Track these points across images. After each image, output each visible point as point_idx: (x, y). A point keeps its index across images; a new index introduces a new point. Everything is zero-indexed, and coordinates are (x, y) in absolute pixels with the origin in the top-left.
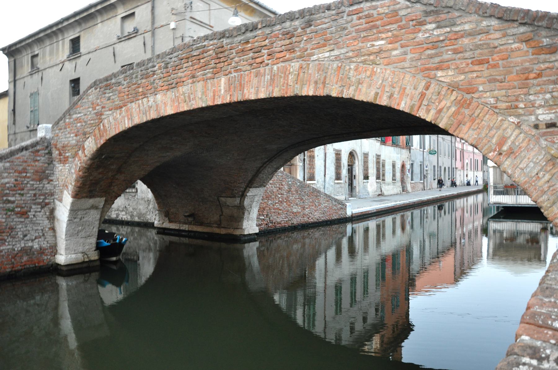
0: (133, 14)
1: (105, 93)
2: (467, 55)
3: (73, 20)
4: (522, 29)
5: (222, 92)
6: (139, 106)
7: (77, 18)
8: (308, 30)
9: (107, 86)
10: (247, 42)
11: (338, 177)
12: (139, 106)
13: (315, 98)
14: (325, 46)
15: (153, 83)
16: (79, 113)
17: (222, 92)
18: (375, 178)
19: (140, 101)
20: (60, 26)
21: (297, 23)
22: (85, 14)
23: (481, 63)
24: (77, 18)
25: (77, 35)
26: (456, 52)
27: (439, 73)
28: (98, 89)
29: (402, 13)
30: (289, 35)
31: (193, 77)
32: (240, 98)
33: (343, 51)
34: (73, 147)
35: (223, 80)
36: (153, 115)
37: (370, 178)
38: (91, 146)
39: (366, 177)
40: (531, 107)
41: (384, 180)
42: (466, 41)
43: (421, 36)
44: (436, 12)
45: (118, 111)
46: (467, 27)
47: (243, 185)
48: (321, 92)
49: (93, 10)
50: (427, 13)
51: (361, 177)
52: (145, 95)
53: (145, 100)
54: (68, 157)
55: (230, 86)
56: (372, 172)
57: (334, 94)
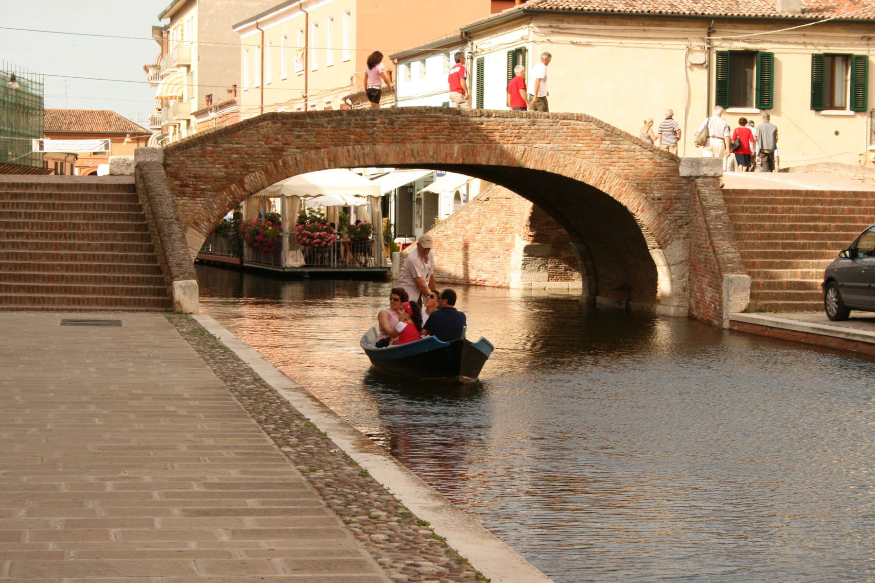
1: (292, 131)
2: (625, 160)
4: (649, 153)
5: (456, 155)
6: (348, 151)
8: (533, 127)
9: (297, 124)
12: (348, 151)
13: (534, 170)
14: (543, 139)
15: (372, 134)
16: (237, 143)
17: (456, 155)
19: (351, 147)
21: (525, 120)
26: (620, 158)
27: (611, 168)
28: (279, 125)
29: (593, 131)
31: (425, 138)
32: (472, 162)
33: (557, 145)
34: (216, 179)
35: (456, 146)
42: (624, 153)
43: (602, 147)
44: (611, 136)
45: (312, 152)
46: (626, 147)
50: (607, 136)
52: (358, 142)
53: (358, 147)
55: (463, 151)
57: (548, 170)
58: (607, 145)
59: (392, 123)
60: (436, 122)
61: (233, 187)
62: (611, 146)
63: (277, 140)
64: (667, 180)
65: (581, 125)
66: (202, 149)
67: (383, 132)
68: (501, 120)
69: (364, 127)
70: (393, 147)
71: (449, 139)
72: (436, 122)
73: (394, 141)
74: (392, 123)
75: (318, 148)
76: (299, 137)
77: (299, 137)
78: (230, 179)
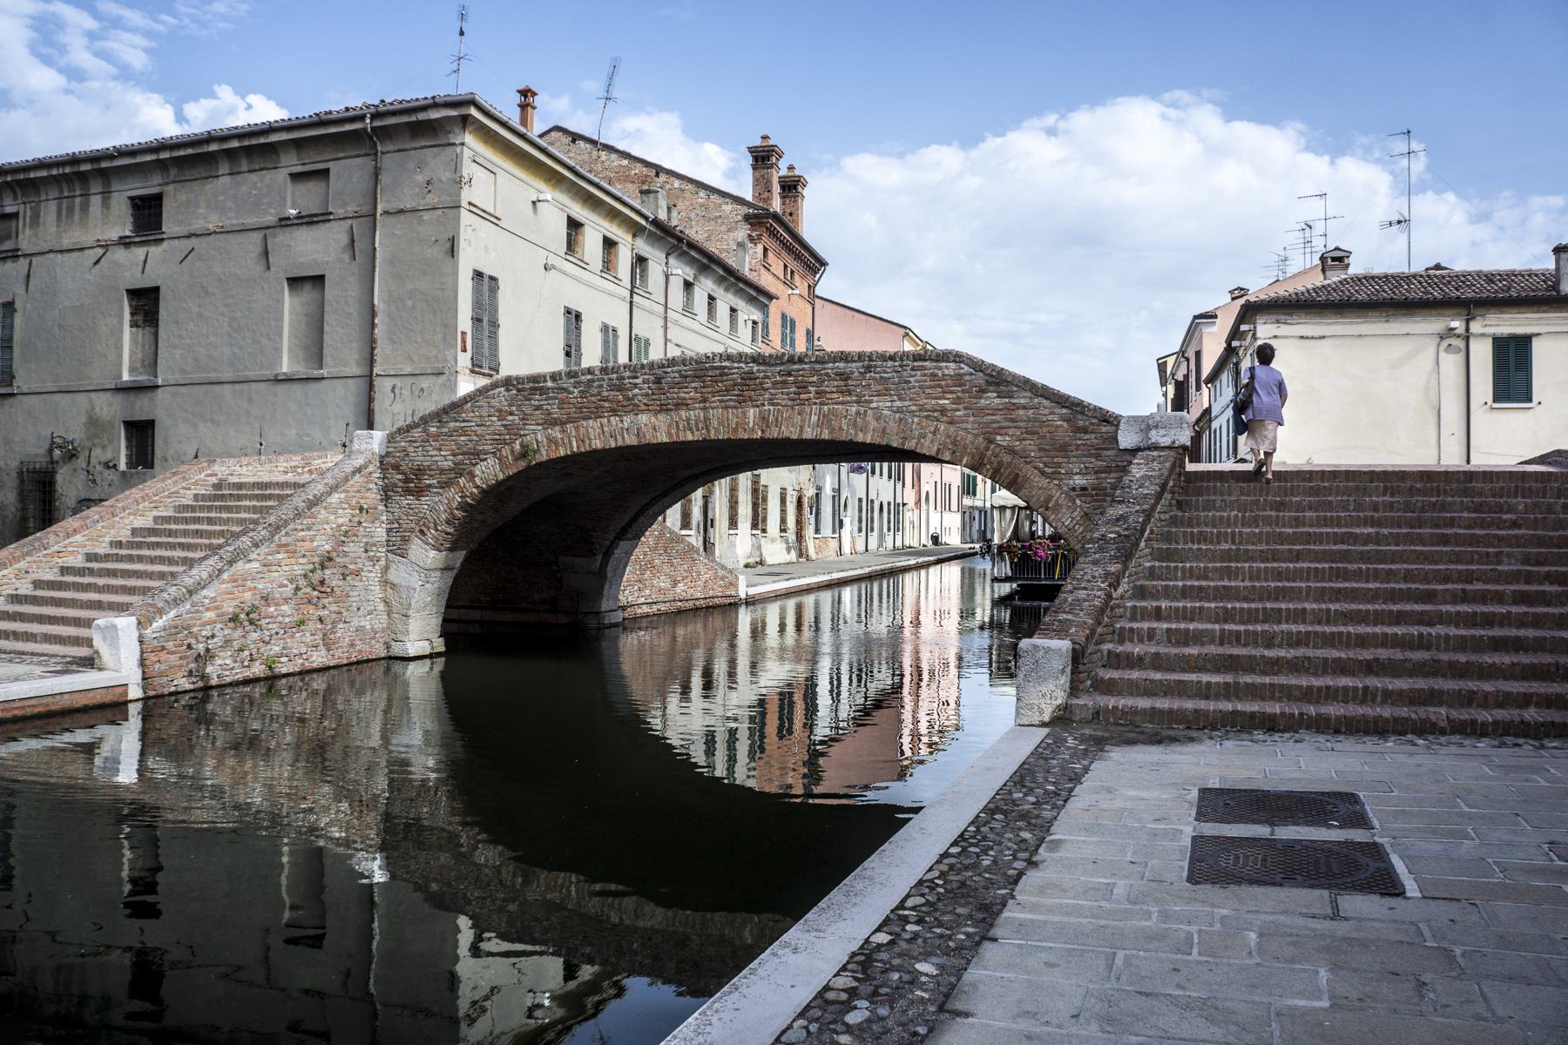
0: (327, 171)
3: (149, 158)
7: (165, 155)
9: (535, 389)
10: (789, 374)
11: (686, 524)
18: (749, 525)
20: (104, 164)
22: (190, 151)
23: (1033, 433)
24: (165, 155)
25: (155, 190)
26: (1013, 420)
30: (844, 376)
34: (442, 471)
36: (631, 440)
37: (740, 525)
38: (489, 471)
39: (733, 523)
40: (1070, 474)
41: (764, 531)
42: (1021, 412)
44: (998, 384)
47: (612, 536)
48: (878, 441)
49: (214, 147)
51: (726, 523)
52: (614, 412)
54: (430, 486)
56: (745, 511)
58: (992, 399)
59: (658, 381)
60: (721, 375)
61: (462, 481)
62: (997, 401)
63: (511, 414)
64: (1098, 457)
65: (950, 368)
66: (425, 431)
67: (647, 395)
68: (818, 366)
69: (620, 389)
70: (661, 417)
71: (742, 401)
72: (721, 375)
73: (664, 409)
74: (658, 381)
75: (563, 423)
76: (538, 408)
77: (538, 408)
78: (458, 470)
